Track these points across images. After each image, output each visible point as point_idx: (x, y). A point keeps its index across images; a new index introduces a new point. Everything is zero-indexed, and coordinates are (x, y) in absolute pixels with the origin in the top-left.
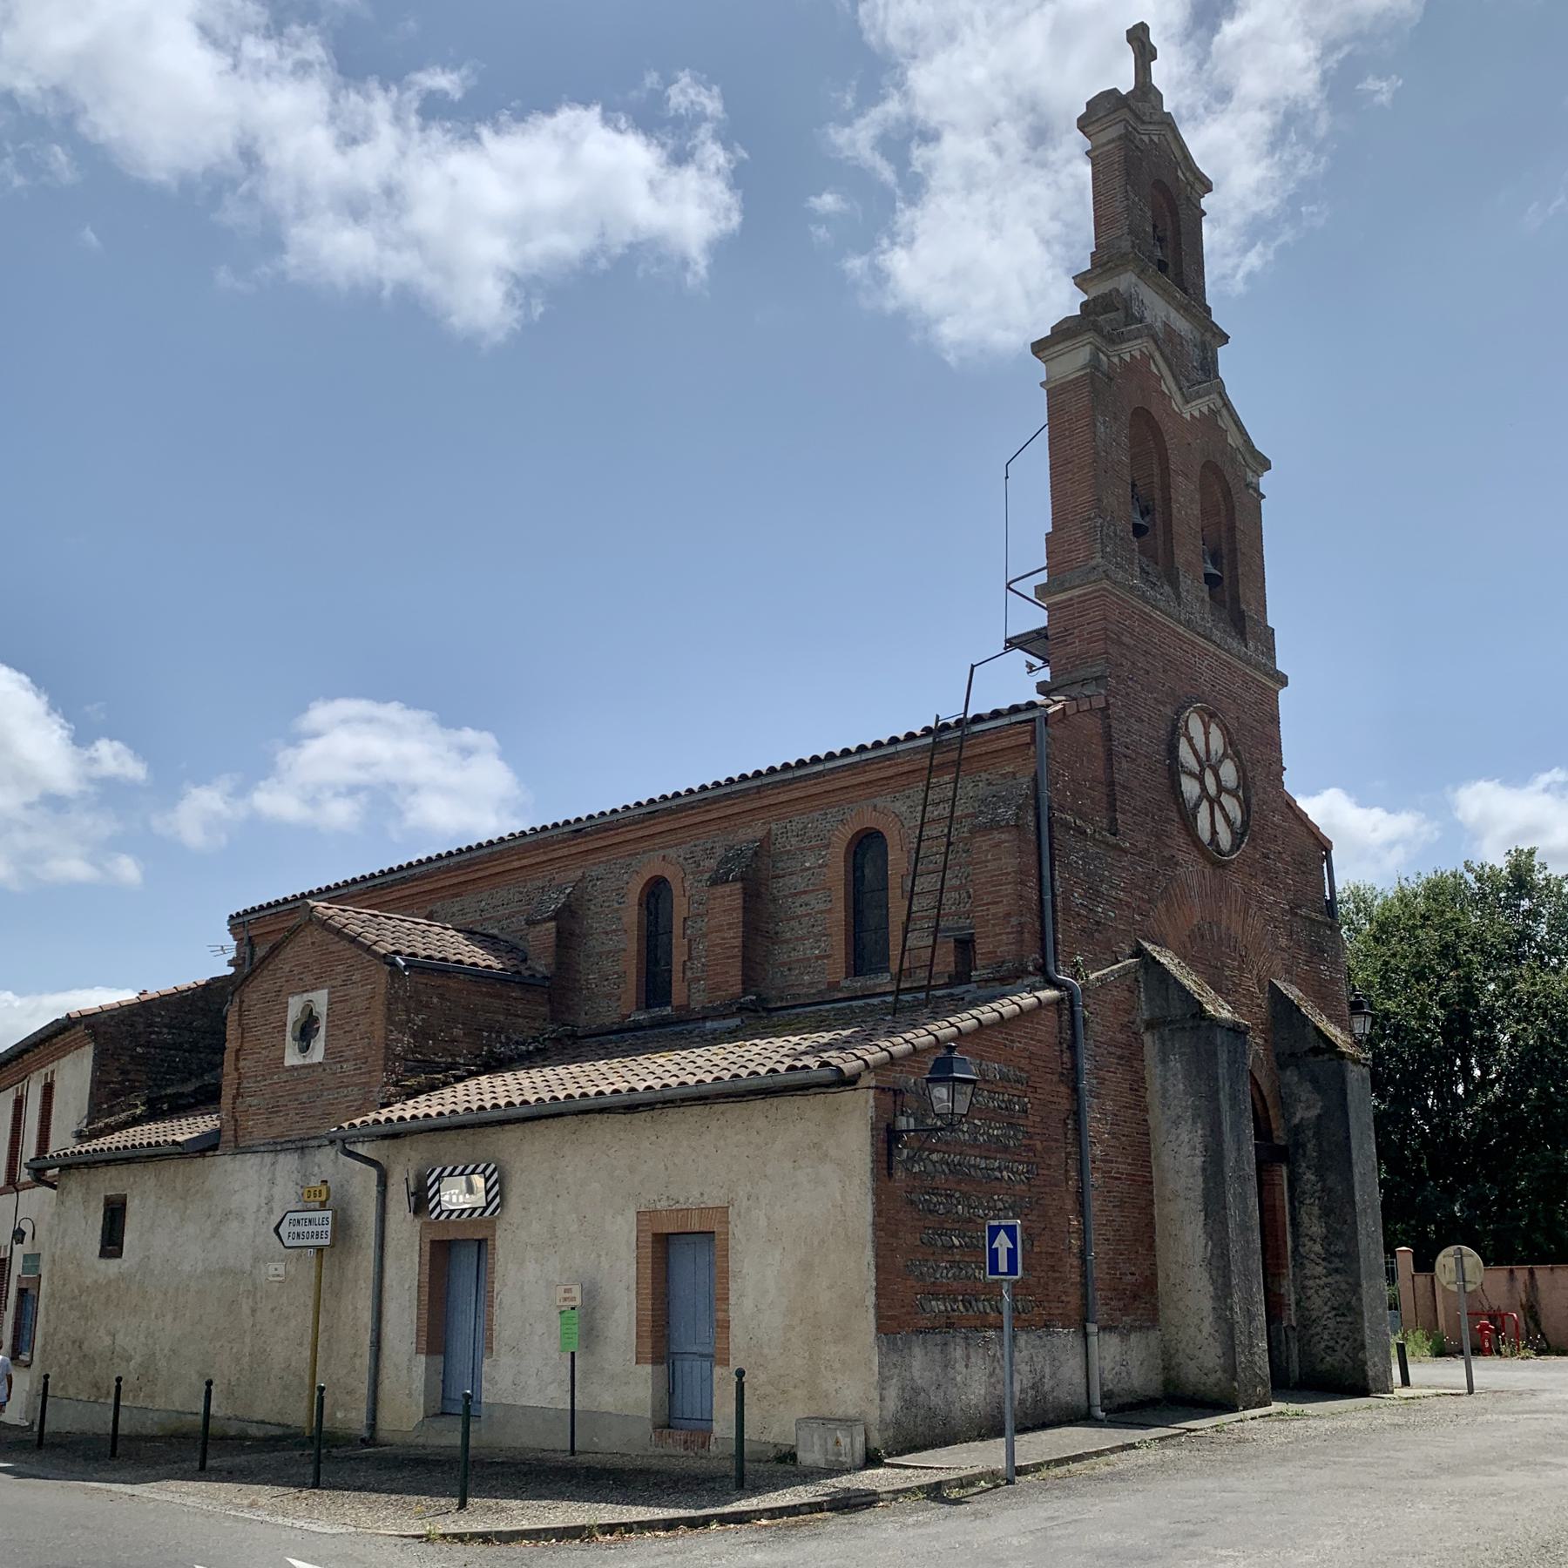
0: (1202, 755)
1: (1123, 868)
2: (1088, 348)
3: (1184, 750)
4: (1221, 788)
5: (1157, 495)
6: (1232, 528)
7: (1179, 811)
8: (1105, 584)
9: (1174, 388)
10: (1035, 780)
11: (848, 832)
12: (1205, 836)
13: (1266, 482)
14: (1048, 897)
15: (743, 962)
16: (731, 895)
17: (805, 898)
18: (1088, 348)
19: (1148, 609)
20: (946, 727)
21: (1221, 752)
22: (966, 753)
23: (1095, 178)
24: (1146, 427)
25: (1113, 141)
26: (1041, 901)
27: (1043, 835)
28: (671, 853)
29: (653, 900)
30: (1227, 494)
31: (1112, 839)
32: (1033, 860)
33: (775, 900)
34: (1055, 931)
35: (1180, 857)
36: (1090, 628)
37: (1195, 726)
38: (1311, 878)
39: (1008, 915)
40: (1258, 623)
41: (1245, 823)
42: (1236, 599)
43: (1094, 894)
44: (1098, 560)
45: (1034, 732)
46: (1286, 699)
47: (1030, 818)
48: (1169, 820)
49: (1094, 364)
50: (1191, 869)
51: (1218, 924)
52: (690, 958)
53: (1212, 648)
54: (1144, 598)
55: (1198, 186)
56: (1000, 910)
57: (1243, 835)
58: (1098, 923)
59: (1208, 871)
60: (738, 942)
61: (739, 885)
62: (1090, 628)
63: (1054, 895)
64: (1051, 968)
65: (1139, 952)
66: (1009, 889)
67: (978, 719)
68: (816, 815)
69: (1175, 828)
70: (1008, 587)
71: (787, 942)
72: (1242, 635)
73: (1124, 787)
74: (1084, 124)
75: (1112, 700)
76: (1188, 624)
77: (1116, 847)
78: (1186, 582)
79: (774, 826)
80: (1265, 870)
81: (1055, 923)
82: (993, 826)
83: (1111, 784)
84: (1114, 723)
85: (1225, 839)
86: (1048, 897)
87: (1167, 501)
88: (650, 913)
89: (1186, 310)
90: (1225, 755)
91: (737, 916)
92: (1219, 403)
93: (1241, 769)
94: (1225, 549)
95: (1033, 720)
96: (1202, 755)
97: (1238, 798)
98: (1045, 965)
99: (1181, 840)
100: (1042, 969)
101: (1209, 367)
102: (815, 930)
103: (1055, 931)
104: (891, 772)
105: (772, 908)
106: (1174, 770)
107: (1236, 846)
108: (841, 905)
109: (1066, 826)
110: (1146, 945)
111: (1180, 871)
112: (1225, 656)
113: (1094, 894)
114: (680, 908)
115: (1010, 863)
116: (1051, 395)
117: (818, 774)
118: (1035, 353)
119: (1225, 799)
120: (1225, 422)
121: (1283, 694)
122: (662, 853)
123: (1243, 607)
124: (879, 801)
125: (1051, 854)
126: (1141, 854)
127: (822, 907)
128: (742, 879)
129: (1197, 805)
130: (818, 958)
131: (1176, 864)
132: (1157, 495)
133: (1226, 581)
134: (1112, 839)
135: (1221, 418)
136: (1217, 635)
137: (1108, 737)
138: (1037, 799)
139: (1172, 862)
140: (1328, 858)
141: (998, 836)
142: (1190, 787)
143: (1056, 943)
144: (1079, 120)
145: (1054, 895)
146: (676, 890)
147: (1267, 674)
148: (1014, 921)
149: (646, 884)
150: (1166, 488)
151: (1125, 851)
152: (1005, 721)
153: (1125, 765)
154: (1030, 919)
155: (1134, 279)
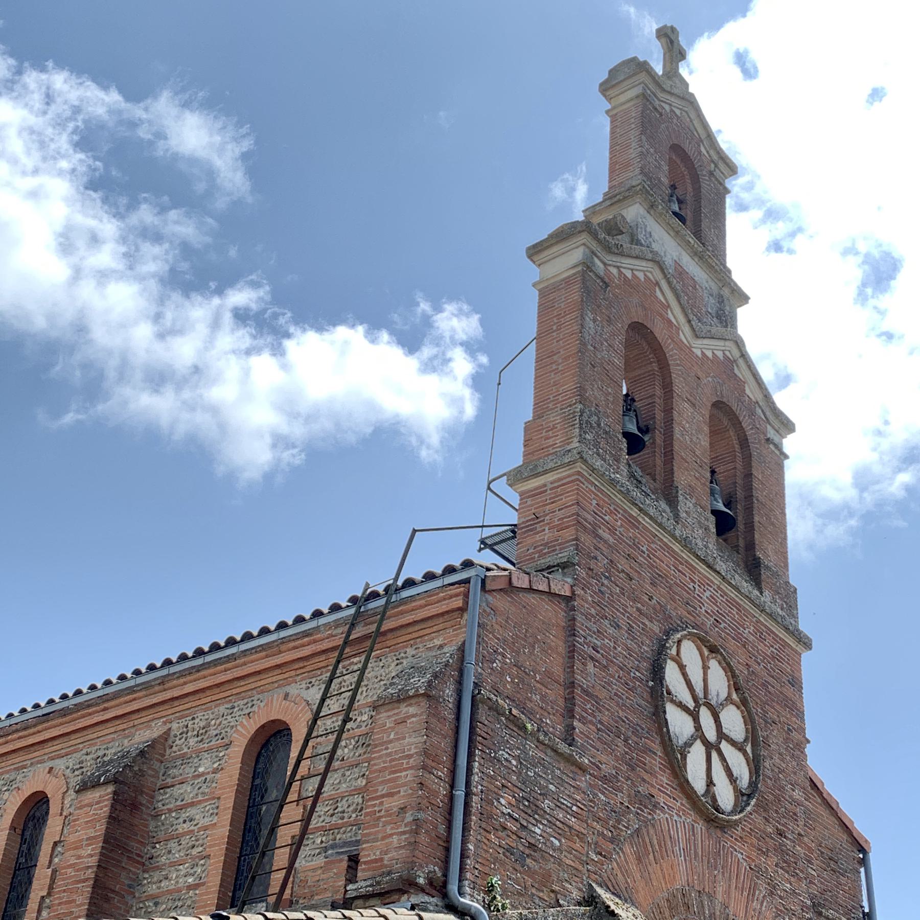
0: (701, 694)
1: (577, 788)
2: (581, 249)
3: (671, 673)
4: (721, 735)
5: (659, 416)
6: (748, 476)
7: (663, 743)
8: (579, 466)
9: (682, 319)
10: (462, 649)
11: (251, 727)
12: (699, 785)
13: (789, 444)
14: (460, 794)
15: (94, 887)
16: (102, 796)
17: (191, 812)
18: (581, 249)
19: (635, 512)
20: (375, 595)
21: (724, 695)
22: (387, 625)
23: (613, 132)
24: (644, 346)
25: (631, 99)
26: (451, 798)
27: (464, 716)
28: (60, 764)
29: (31, 824)
30: (744, 443)
31: (563, 747)
32: (445, 744)
33: (157, 816)
34: (464, 842)
35: (661, 799)
36: (560, 514)
37: (690, 652)
38: (843, 880)
39: (403, 809)
40: (776, 575)
41: (753, 784)
42: (751, 546)
43: (530, 807)
44: (575, 444)
45: (466, 595)
46: (810, 666)
47: (449, 692)
48: (648, 750)
49: (587, 266)
50: (676, 820)
51: (711, 897)
52: (49, 894)
53: (717, 580)
54: (626, 494)
55: (722, 166)
56: (394, 804)
57: (750, 796)
58: (531, 846)
59: (700, 826)
60: (93, 861)
61: (110, 789)
62: (560, 514)
63: (468, 794)
64: (453, 888)
65: (591, 900)
66: (408, 776)
67: (409, 583)
68: (222, 709)
69: (656, 761)
70: (489, 488)
71: (158, 868)
72: (757, 582)
73: (585, 691)
74: (605, 88)
75: (579, 591)
76: (685, 543)
77: (569, 760)
78: (686, 505)
79: (175, 726)
80: (781, 850)
81: (465, 829)
82: (402, 698)
83: (571, 685)
84: (580, 618)
85: (726, 797)
86: (460, 794)
87: (669, 422)
88: (23, 841)
89: (701, 258)
90: (729, 699)
91: (100, 828)
92: (736, 353)
93: (749, 720)
94: (740, 494)
95: (467, 581)
96: (701, 694)
97: (745, 753)
98: (445, 884)
99: (664, 778)
100: (439, 888)
101: (727, 320)
102: (194, 852)
103: (464, 842)
104: (306, 651)
105: (152, 825)
106: (658, 694)
107: (739, 807)
108: (227, 816)
109: (496, 709)
110: (600, 891)
111: (659, 815)
112: (733, 594)
113: (530, 807)
114: (53, 828)
115: (413, 742)
116: (543, 294)
117: (233, 657)
118: (530, 257)
119: (725, 746)
120: (741, 372)
121: (806, 657)
122: (50, 764)
123: (759, 554)
124: (293, 690)
125: (471, 740)
126: (605, 779)
127: (206, 821)
128: (115, 781)
129: (689, 744)
130: (190, 887)
131: (656, 806)
132: (659, 416)
133: (741, 525)
134: (563, 747)
135: (736, 365)
136: (721, 566)
137: (571, 631)
138: (461, 672)
139: (648, 802)
140: (864, 862)
141: (406, 709)
142: (679, 724)
143: (463, 856)
144: (601, 85)
145: (468, 794)
146: (54, 808)
147: (787, 629)
148: (409, 818)
149: (25, 802)
150: (668, 410)
151: (582, 769)
152: (437, 583)
153: (590, 667)
154: (433, 818)
155: (642, 211)
